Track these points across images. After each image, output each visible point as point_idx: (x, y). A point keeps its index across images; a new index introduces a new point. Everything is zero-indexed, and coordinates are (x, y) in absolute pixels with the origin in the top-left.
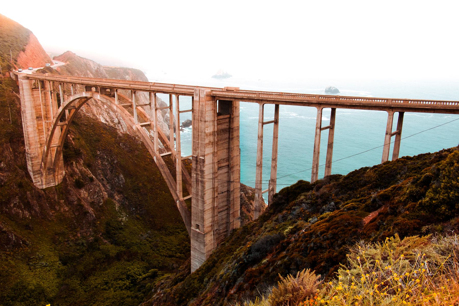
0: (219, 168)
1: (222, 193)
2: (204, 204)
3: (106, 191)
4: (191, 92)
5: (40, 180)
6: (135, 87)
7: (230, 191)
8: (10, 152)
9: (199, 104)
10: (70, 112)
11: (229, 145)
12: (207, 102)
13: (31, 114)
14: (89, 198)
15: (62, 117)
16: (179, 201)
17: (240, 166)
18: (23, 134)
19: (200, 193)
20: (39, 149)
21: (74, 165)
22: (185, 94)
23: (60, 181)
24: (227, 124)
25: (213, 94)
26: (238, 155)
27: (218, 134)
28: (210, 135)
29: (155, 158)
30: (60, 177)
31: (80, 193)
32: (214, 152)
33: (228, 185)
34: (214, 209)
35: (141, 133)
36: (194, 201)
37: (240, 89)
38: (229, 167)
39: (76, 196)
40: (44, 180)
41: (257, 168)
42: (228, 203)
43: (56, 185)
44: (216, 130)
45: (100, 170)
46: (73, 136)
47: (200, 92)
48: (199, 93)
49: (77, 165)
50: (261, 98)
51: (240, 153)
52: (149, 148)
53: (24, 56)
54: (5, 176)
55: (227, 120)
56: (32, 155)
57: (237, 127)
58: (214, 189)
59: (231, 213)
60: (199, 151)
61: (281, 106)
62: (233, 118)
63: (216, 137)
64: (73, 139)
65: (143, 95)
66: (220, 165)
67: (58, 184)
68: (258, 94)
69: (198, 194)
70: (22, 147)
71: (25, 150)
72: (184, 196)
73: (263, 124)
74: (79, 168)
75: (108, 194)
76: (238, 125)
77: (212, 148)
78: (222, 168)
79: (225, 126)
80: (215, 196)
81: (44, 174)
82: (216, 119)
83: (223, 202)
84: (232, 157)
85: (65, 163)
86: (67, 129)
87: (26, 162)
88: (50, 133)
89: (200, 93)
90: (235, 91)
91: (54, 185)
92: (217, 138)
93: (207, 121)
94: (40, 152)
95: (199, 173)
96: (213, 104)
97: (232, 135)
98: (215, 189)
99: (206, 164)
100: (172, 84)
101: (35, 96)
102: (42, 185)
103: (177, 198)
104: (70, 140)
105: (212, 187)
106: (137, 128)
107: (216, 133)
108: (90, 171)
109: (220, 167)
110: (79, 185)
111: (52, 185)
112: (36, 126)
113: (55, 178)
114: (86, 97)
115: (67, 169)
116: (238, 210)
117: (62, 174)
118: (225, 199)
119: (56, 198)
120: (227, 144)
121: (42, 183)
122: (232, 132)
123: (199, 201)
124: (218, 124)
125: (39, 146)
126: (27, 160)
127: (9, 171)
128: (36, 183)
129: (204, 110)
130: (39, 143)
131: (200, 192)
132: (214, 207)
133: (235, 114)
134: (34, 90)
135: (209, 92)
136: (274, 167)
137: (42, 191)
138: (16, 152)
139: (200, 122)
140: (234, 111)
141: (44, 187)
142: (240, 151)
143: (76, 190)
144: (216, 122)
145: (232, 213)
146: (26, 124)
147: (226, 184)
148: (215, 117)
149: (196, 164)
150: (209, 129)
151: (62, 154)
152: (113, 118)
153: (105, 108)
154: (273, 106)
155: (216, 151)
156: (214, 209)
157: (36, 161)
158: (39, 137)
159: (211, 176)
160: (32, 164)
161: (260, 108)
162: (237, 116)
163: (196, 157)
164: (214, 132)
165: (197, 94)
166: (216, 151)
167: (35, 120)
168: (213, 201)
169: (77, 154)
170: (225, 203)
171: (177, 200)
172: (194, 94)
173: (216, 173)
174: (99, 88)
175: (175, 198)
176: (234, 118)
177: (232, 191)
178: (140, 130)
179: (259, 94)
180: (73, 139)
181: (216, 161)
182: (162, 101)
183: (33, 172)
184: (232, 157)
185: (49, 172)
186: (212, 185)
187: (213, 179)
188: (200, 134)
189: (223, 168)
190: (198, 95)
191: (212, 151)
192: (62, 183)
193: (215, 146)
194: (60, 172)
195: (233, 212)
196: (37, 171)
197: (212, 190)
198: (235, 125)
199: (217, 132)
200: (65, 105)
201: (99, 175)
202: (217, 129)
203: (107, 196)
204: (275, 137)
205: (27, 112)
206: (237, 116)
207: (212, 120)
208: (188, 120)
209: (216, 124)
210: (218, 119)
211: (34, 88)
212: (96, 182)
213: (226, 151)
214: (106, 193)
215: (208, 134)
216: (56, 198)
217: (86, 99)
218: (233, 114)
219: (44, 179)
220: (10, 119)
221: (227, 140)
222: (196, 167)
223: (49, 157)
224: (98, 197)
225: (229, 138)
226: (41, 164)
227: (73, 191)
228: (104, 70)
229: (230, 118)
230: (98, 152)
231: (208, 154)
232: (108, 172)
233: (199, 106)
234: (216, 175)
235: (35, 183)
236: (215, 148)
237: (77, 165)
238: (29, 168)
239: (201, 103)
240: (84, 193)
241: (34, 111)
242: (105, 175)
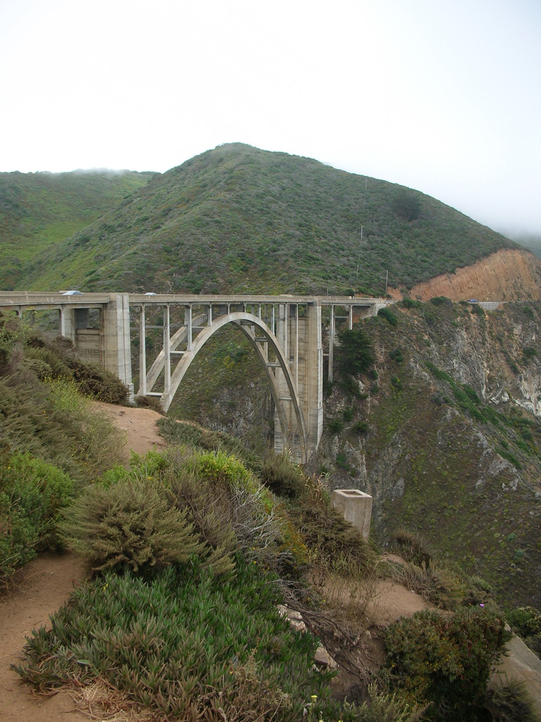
5: (282, 448)
24: (96, 344)
45: (385, 464)
57: (114, 351)
64: (373, 406)
104: (366, 406)
108: (366, 460)
117: (314, 449)
169: (361, 430)
180: (373, 406)
194: (311, 446)
201: (376, 471)
206: (113, 336)
207: (70, 332)
232: (390, 471)
242: (385, 475)
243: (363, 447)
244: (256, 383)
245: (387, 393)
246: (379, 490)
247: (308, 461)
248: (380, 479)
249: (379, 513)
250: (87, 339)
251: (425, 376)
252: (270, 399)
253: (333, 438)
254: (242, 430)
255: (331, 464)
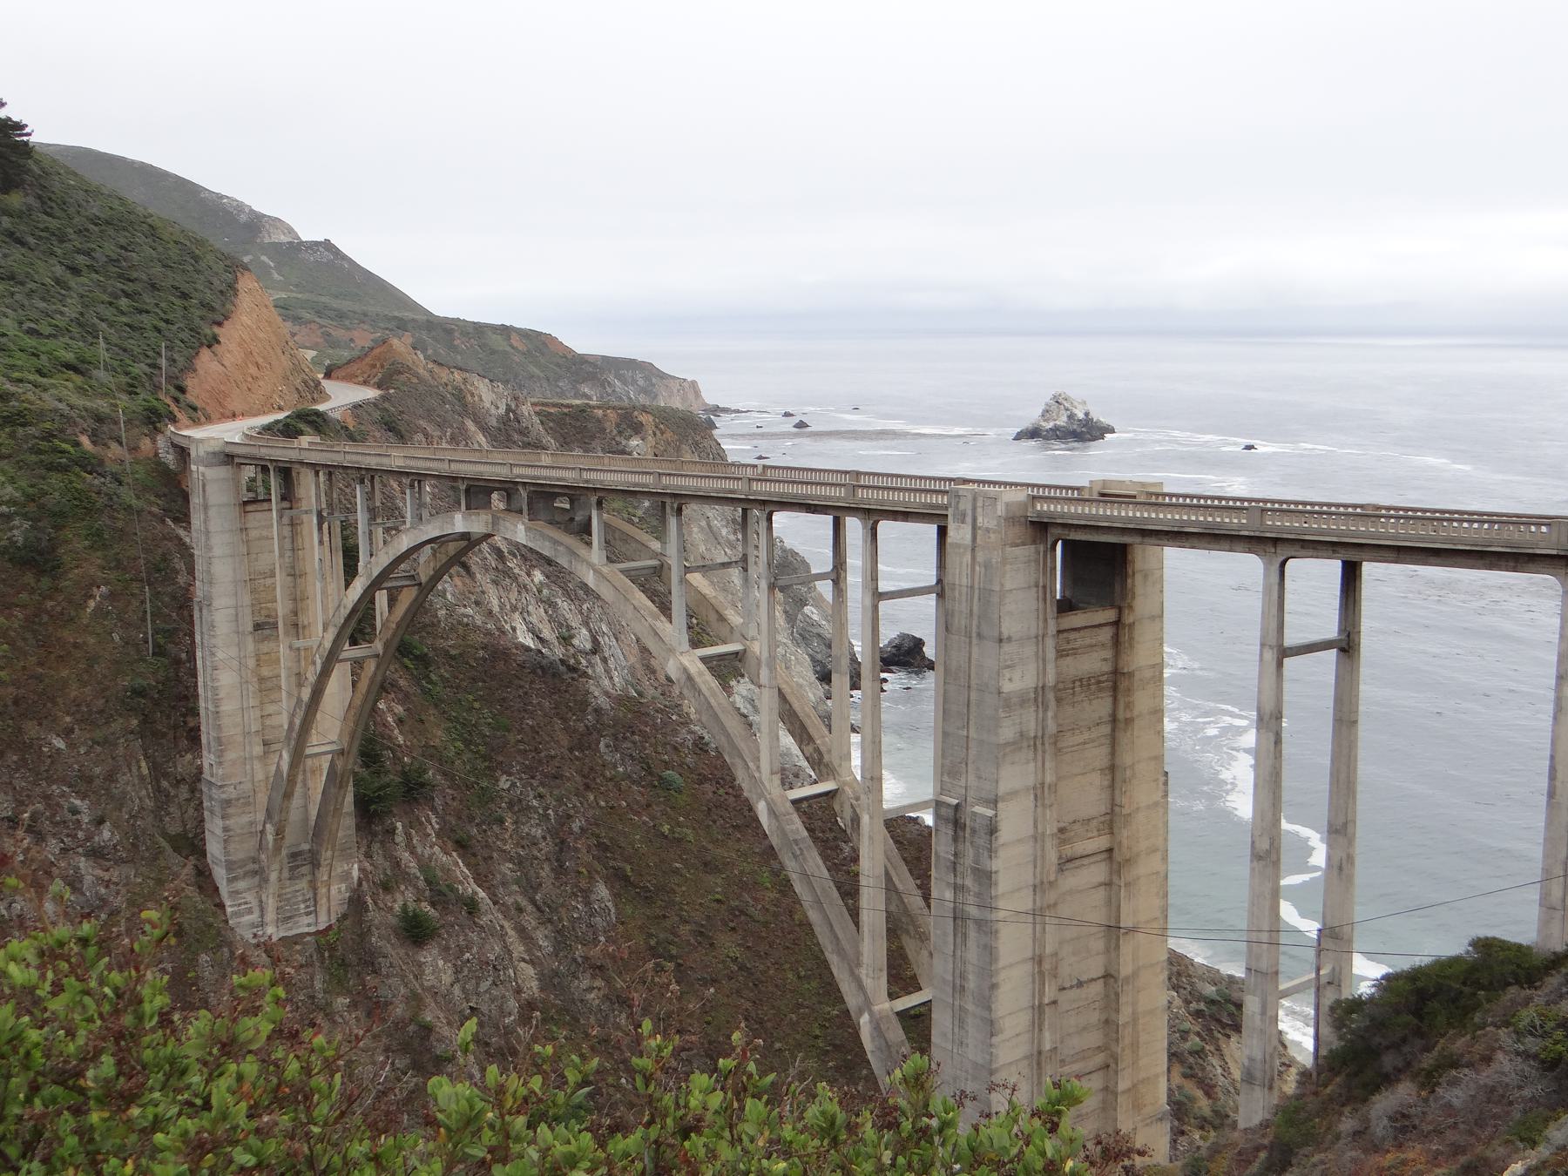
0: (1066, 863)
1: (1080, 984)
2: (992, 1035)
3: (531, 962)
4: (932, 506)
5: (254, 904)
6: (681, 487)
7: (1116, 980)
8: (142, 778)
9: (974, 558)
10: (392, 601)
11: (1113, 753)
12: (1008, 549)
13: (232, 611)
14: (457, 990)
15: (358, 626)
16: (871, 1014)
17: (1165, 859)
18: (196, 696)
19: (971, 984)
20: (257, 765)
21: (400, 838)
22: (906, 516)
23: (338, 909)
25: (1040, 514)
26: (1156, 804)
27: (1059, 700)
28: (1023, 702)
29: (761, 809)
30: (337, 893)
31: (420, 965)
32: (1043, 784)
33: (1107, 950)
34: (1039, 1064)
35: (700, 692)
36: (941, 1023)
37: (1166, 490)
38: (1110, 858)
39: (403, 977)
40: (271, 904)
41: (1253, 869)
42: (1106, 1035)
43: (322, 927)
44: (1051, 679)
45: (511, 860)
46: (399, 709)
47: (979, 504)
48: (974, 509)
49: (409, 837)
50: (1272, 528)
51: (1166, 795)
52: (738, 761)
53: (215, 366)
54: (117, 884)
55: (1106, 635)
56: (231, 793)
57: (1153, 666)
58: (1040, 963)
59: (1123, 1085)
60: (972, 780)
61: (1371, 571)
62: (1132, 626)
63: (1050, 714)
65: (703, 523)
66: (1068, 851)
67: (330, 927)
68: (1258, 514)
69: (963, 988)
70: (189, 756)
71: (200, 769)
72: (892, 996)
73: (1284, 653)
74: (419, 850)
75: (541, 977)
76: (1159, 661)
77: (1032, 765)
78: (1077, 863)
79: (1094, 662)
80: (1046, 1001)
81: (273, 876)
82: (1052, 629)
83: (1084, 1029)
84: (1125, 811)
85: (358, 828)
86: (379, 678)
87: (203, 821)
88: (306, 694)
89: (979, 510)
90: (1141, 499)
91: (312, 929)
92: (1055, 717)
93: (1009, 639)
94: (260, 776)
95: (969, 882)
96: (1037, 561)
97: (1128, 706)
98: (1046, 966)
99: (1001, 841)
100: (846, 472)
101: (253, 534)
102: (262, 924)
103: (861, 999)
105: (1029, 954)
106: (685, 670)
107: (1051, 696)
108: (467, 865)
109: (1070, 860)
110: (416, 932)
111: (304, 925)
112: (251, 663)
113: (315, 894)
114: (465, 536)
115: (368, 856)
116: (1157, 1076)
117: (347, 876)
118: (1095, 1017)
119: (318, 985)
120: (1105, 750)
121: (262, 916)
122: (1129, 690)
123: (970, 1020)
124: (1061, 654)
125: (258, 749)
126: (206, 813)
127: (132, 861)
128: (236, 914)
129: (997, 588)
130: (258, 740)
131: (971, 977)
132: (1040, 1053)
133: (1142, 605)
134: (249, 508)
135: (1019, 503)
136: (1340, 868)
137: (260, 952)
138: (166, 775)
139: (975, 641)
140: (1139, 590)
141: (273, 932)
142: (1166, 783)
143: (402, 952)
144: (1050, 643)
145: (1129, 1090)
146: (213, 654)
147: (1098, 945)
148: (1046, 620)
149: (955, 839)
150: (1017, 675)
151: (351, 788)
152: (569, 628)
153: (536, 580)
154: (1331, 569)
155: (1049, 779)
156: (1039, 1064)
157: (245, 819)
158: (258, 713)
159: (1025, 902)
160: (226, 829)
161: (1266, 575)
162: (1153, 618)
163: (958, 805)
164: (1041, 690)
165: (964, 515)
166: (1049, 779)
167: (250, 639)
168: (1037, 1024)
169: (414, 791)
170: (1094, 1038)
171: (861, 1013)
172: (950, 512)
173: (1050, 883)
174: (524, 494)
175: (852, 1000)
176: (1137, 626)
177: (1127, 979)
178: (698, 680)
179: (1264, 510)
180: (400, 722)
181: (1051, 828)
182: (784, 550)
183: (230, 866)
184: (1125, 811)
185: (292, 869)
186: (1030, 942)
187: (1037, 914)
188: (974, 696)
189: (1085, 861)
190: (969, 519)
191: (1031, 781)
192: (344, 917)
193: (1048, 757)
194: (339, 870)
195: (1134, 1086)
196: (243, 863)
197: (1028, 967)
198: (1138, 659)
199: (1055, 688)
200: (375, 574)
202: (1058, 674)
203: (535, 984)
204: (1345, 718)
205: (216, 603)
206: (1153, 618)
207: (1033, 632)
208: (903, 637)
209: (1051, 654)
210: (1063, 627)
211: (251, 502)
212: (490, 915)
213: (1097, 781)
214: (530, 971)
215: (1015, 700)
216: (318, 985)
217: (464, 543)
218: (1131, 607)
219: (271, 901)
220: (146, 633)
221: (1106, 729)
222: (956, 855)
223: (296, 801)
224: (494, 983)
225: (1114, 720)
226: (263, 832)
227: (392, 951)
228: (537, 414)
229: (1117, 623)
230: (504, 777)
231: (1014, 794)
232: (543, 874)
233: (973, 570)
234: (1051, 897)
235: (235, 914)
236: (1048, 765)
237: (409, 837)
238: (214, 848)
239: (980, 556)
240: (435, 966)
241: (247, 599)
242: (530, 887)
243: (438, 836)
244: (67, 733)
245: (402, 682)
246: (535, 929)
247: (333, 921)
248: (519, 899)
249: (585, 983)
250: (1079, 643)
251: (467, 616)
252: (145, 771)
253: (391, 832)
254: (103, 891)
255: (418, 900)
